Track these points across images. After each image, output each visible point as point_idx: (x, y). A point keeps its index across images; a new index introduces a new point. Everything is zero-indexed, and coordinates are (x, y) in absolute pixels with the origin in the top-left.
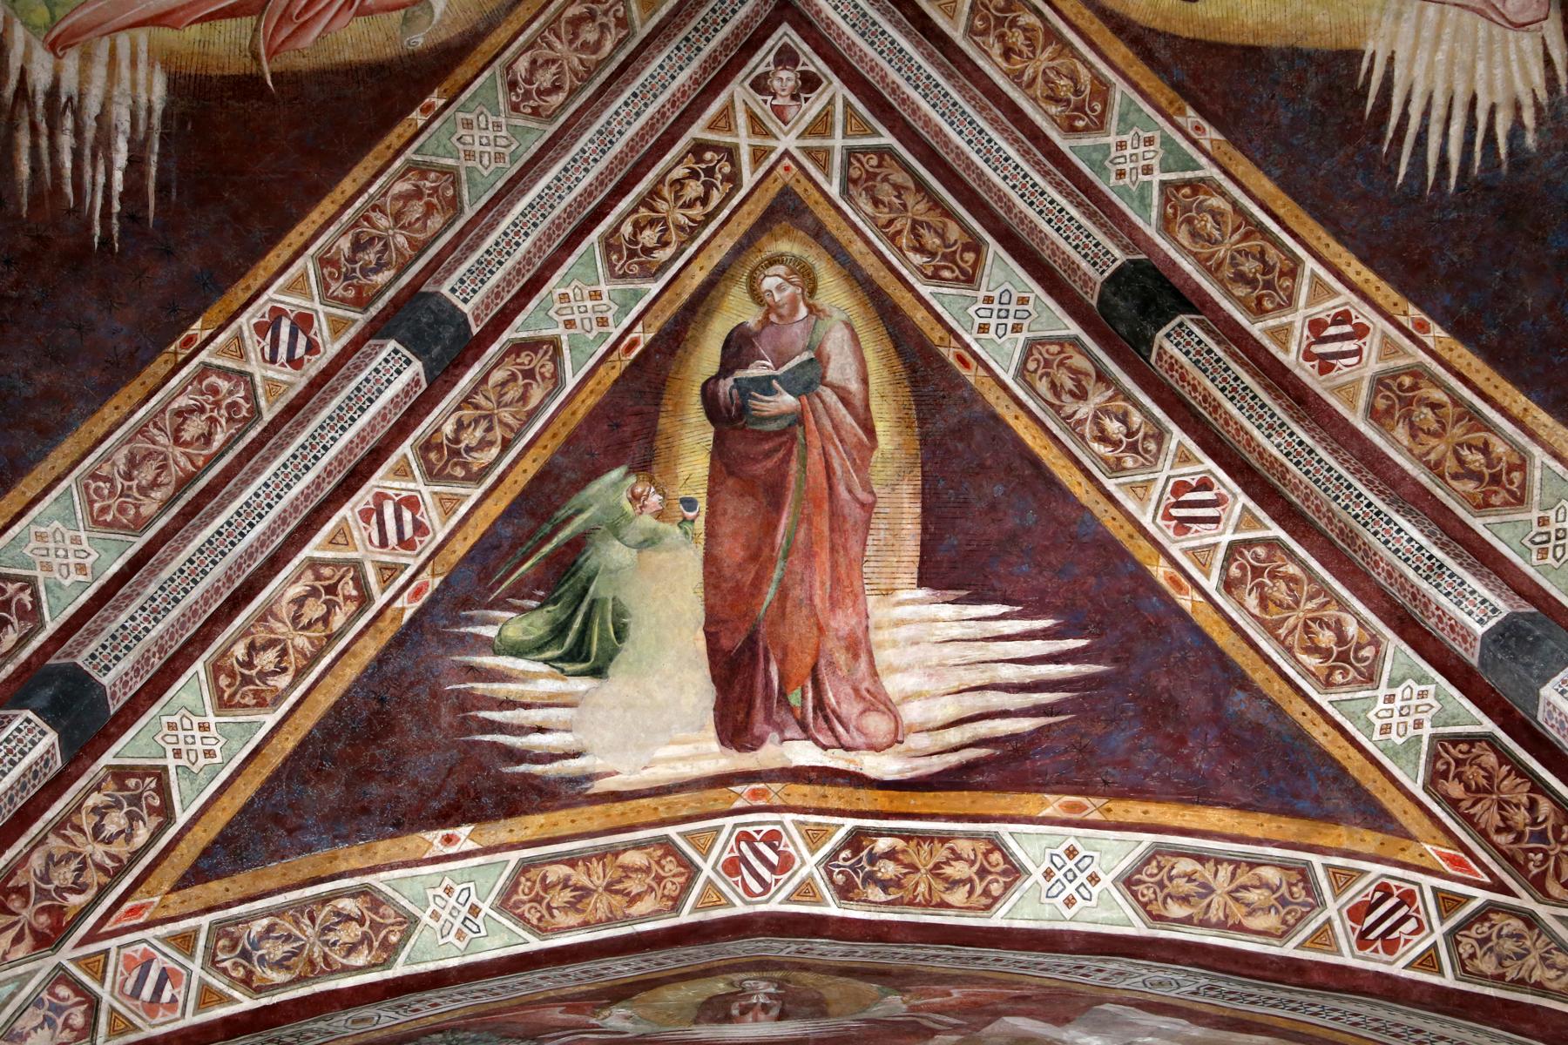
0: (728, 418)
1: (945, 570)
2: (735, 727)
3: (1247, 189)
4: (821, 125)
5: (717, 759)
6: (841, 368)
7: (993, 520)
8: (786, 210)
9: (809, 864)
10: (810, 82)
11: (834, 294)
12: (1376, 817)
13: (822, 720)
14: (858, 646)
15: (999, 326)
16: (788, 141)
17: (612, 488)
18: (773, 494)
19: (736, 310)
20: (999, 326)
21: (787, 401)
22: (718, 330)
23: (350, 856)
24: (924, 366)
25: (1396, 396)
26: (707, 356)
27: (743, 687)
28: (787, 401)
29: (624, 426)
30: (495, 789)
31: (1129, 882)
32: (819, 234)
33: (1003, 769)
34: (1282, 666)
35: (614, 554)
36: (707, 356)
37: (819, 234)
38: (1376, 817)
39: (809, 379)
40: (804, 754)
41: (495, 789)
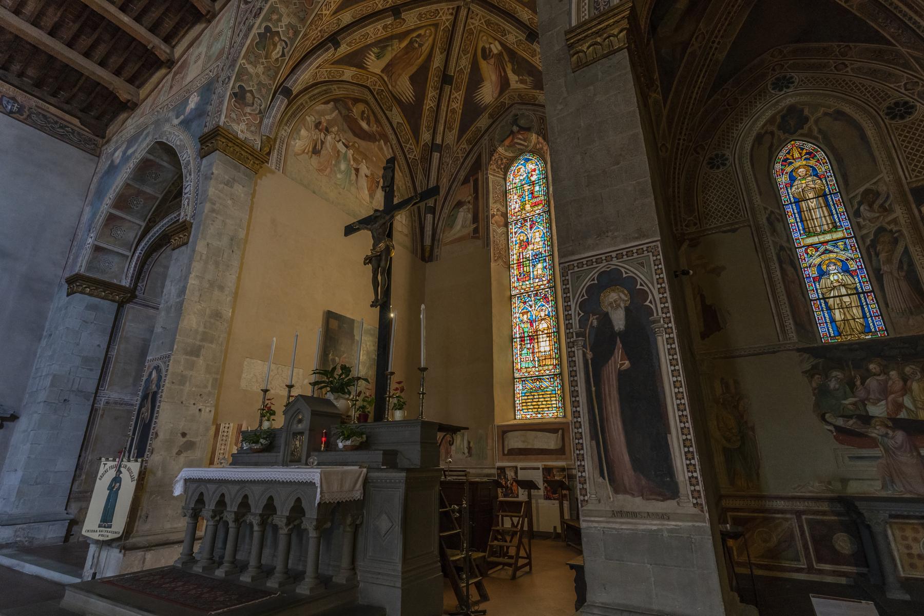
0: (411, 42)
1: (412, 79)
2: (382, 71)
3: (465, 78)
4: (447, 20)
5: (378, 71)
6: (424, 48)
7: (419, 80)
8: (436, 25)
9: (377, 87)
10: (452, 14)
11: (431, 39)
12: (417, 143)
13: (390, 77)
14: (400, 75)
15: (437, 62)
16: (444, 18)
17: (396, 41)
18: (407, 53)
19: (422, 32)
20: (437, 62)
21: (417, 45)
22: (417, 33)
23: (345, 67)
24: (430, 57)
25: (454, 111)
26: (415, 35)
27: (388, 69)
28: (417, 45)
29: (401, 36)
30: (361, 66)
31: (398, 123)
32: (436, 31)
33: (399, 102)
34: (424, 122)
35: (390, 48)
36: (415, 35)
37: (436, 31)
38: (417, 143)
39: (421, 45)
40: (386, 79)
41: (361, 66)
